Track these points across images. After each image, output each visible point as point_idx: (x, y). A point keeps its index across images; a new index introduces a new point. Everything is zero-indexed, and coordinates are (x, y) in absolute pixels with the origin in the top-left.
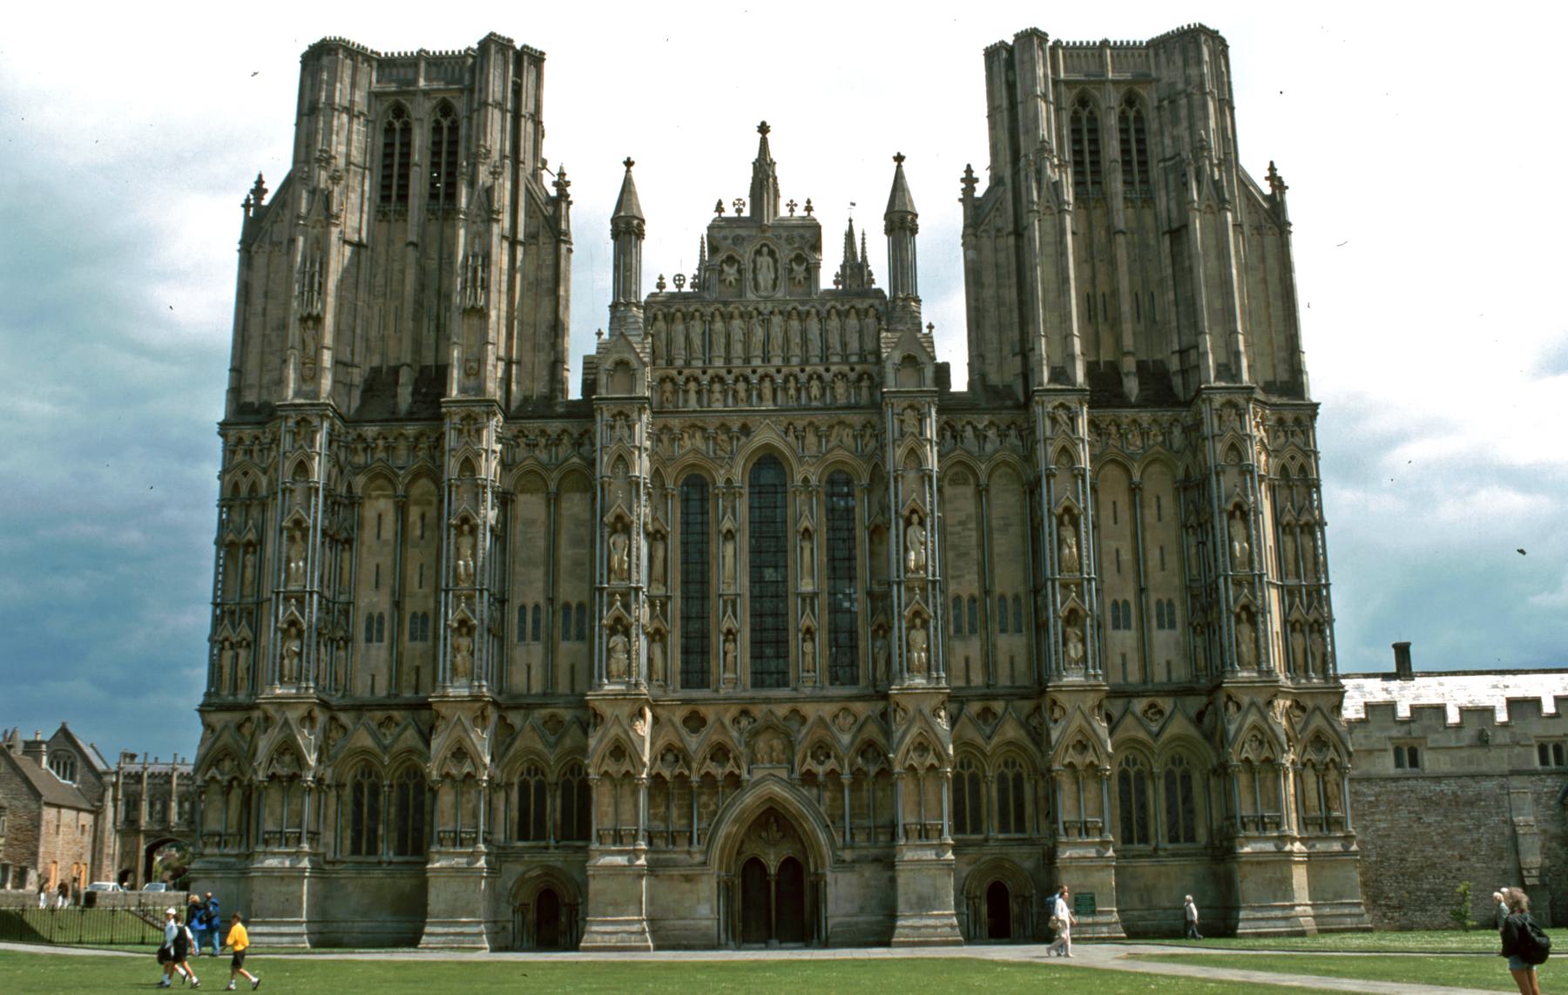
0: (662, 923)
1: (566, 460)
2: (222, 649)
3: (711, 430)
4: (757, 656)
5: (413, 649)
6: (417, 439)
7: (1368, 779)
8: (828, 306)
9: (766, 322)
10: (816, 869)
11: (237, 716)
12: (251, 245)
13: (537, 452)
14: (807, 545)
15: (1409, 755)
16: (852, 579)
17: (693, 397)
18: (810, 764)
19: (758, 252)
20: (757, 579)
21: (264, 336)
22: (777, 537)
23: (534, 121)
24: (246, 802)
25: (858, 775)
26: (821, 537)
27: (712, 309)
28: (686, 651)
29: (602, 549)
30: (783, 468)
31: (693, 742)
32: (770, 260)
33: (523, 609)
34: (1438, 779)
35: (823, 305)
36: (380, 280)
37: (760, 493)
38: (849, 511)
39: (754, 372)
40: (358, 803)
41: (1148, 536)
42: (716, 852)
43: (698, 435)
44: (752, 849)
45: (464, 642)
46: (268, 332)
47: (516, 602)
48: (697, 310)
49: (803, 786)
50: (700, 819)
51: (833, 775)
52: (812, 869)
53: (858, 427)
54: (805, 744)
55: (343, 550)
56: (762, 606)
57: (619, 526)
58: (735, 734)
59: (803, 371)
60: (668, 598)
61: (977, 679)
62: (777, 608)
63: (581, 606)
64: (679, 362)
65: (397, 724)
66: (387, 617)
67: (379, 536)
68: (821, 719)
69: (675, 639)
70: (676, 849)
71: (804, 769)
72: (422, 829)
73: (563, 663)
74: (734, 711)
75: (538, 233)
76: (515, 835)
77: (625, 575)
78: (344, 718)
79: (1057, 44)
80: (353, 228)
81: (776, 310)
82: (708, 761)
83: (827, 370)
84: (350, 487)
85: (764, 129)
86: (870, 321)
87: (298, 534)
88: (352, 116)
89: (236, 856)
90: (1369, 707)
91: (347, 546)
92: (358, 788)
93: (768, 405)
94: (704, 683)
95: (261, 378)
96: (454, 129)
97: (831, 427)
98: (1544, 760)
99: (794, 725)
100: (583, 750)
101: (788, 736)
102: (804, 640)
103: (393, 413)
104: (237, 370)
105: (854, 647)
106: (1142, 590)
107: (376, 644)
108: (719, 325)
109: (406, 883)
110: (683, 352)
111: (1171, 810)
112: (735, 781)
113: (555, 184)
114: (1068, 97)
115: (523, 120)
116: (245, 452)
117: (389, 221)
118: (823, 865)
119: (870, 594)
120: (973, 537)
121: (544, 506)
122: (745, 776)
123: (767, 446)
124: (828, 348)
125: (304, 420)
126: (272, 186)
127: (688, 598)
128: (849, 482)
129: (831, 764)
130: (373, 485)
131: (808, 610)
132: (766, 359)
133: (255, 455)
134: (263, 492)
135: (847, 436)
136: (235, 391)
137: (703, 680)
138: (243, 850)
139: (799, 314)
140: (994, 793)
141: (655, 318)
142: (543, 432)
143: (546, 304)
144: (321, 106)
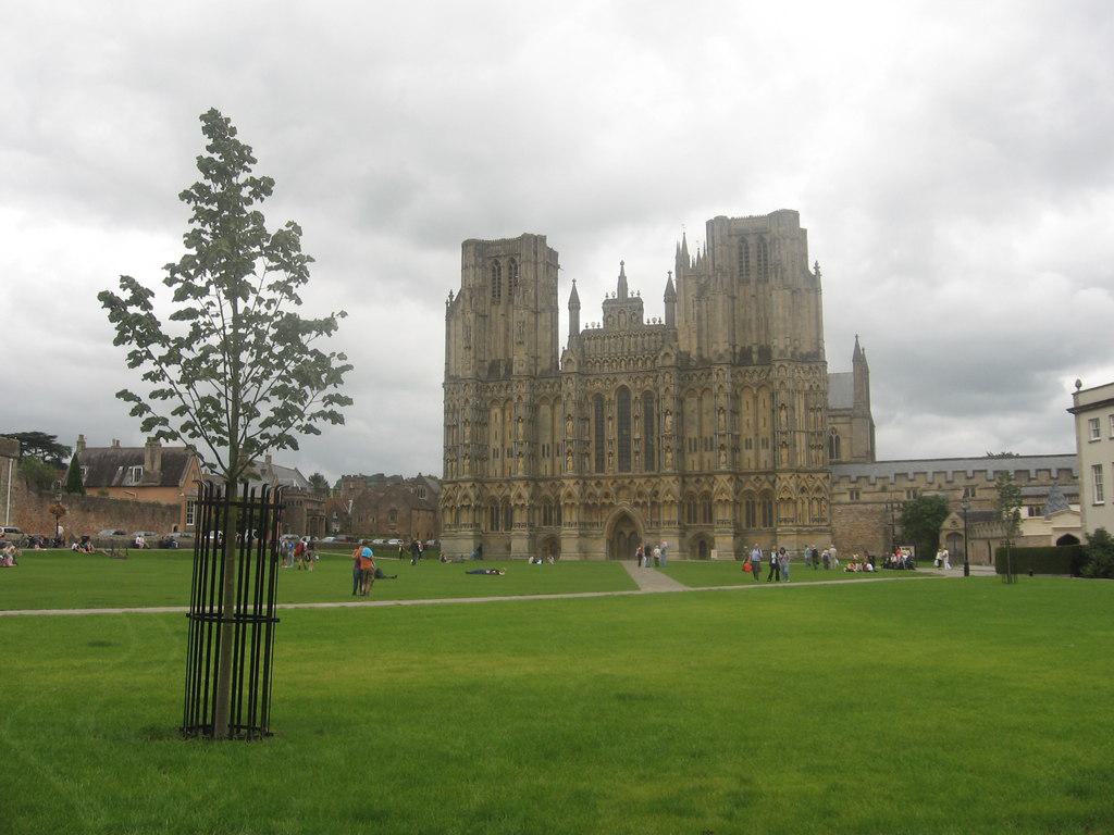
5: (509, 461)
7: (839, 504)
15: (855, 493)
17: (598, 368)
18: (638, 499)
19: (620, 313)
24: (457, 514)
25: (653, 503)
31: (599, 492)
33: (544, 446)
34: (865, 503)
40: (492, 513)
41: (760, 415)
45: (521, 460)
61: (697, 468)
69: (593, 455)
73: (557, 463)
79: (733, 218)
85: (622, 263)
86: (660, 337)
90: (842, 477)
92: (492, 508)
93: (623, 369)
94: (603, 471)
96: (516, 268)
98: (909, 497)
101: (629, 489)
106: (757, 435)
111: (764, 516)
114: (735, 240)
120: (696, 417)
126: (455, 294)
134: (457, 407)
135: (650, 381)
140: (702, 509)
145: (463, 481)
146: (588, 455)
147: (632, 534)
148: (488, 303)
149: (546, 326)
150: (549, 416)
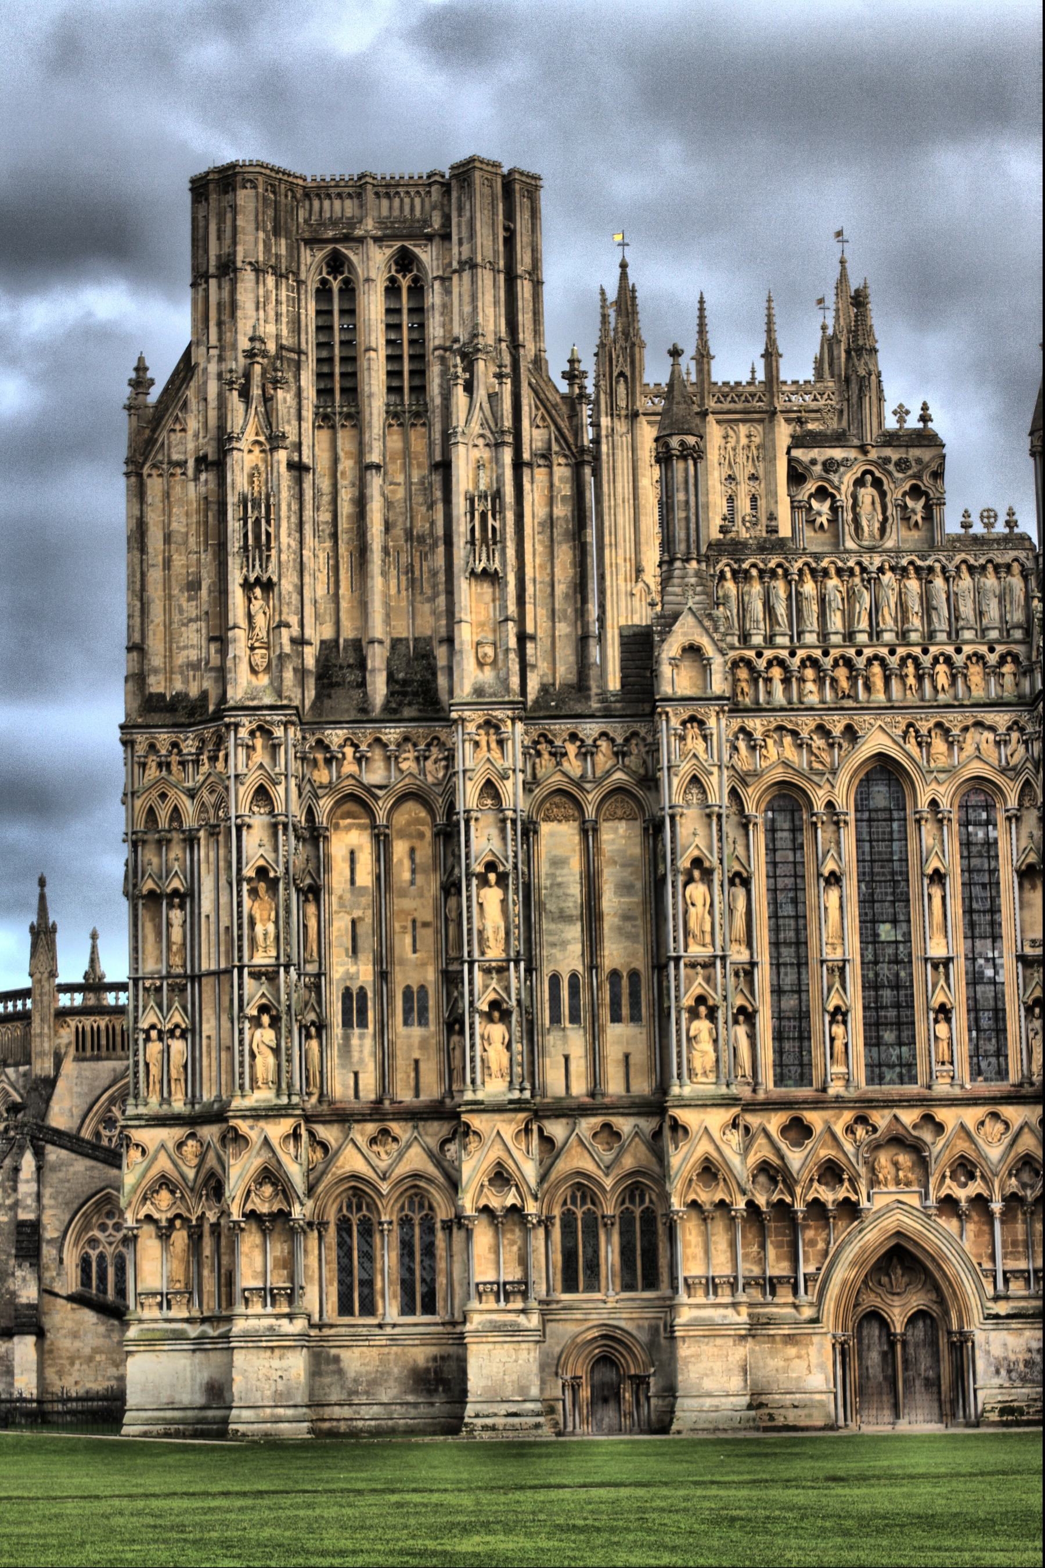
0: (764, 1399)
1: (608, 773)
2: (148, 1039)
3: (804, 734)
4: (872, 1041)
6: (398, 745)
8: (958, 558)
9: (872, 581)
10: (961, 1327)
11: (178, 1133)
12: (144, 464)
13: (566, 765)
14: (936, 892)
16: (996, 938)
17: (778, 688)
18: (951, 1188)
19: (859, 482)
20: (869, 938)
21: (169, 597)
22: (895, 882)
23: (532, 281)
25: (1012, 1200)
26: (955, 883)
27: (799, 564)
28: (779, 1036)
29: (675, 905)
30: (900, 785)
31: (795, 1158)
32: (875, 493)
33: (555, 980)
35: (950, 559)
36: (325, 516)
37: (870, 820)
38: (991, 845)
39: (859, 653)
40: (344, 1247)
42: (830, 1305)
43: (788, 740)
44: (871, 1300)
45: (497, 1031)
46: (175, 592)
47: (547, 971)
48: (779, 565)
49: (939, 1216)
50: (806, 1260)
51: (980, 1202)
52: (955, 1327)
53: (1002, 730)
54: (945, 1159)
55: (306, 900)
56: (877, 975)
57: (696, 874)
58: (849, 1148)
59: (925, 651)
60: (753, 964)
62: (897, 975)
63: (634, 975)
64: (757, 640)
65: (395, 1140)
66: (370, 995)
67: (353, 881)
68: (962, 1126)
69: (765, 1022)
70: (777, 1300)
71: (943, 1193)
72: (433, 1280)
74: (848, 1116)
75: (550, 448)
76: (559, 1285)
77: (708, 939)
78: (324, 1132)
80: (293, 444)
81: (887, 567)
82: (816, 1184)
83: (959, 651)
84: (310, 813)
86: (1016, 582)
87: (262, 886)
88: (279, 276)
89: (188, 1320)
91: (310, 896)
92: (344, 1226)
93: (880, 697)
94: (804, 1079)
95: (169, 655)
96: (417, 290)
97: (966, 729)
99: (927, 1136)
100: (662, 1175)
101: (917, 1149)
102: (936, 1021)
103: (364, 710)
104: (137, 648)
105: (1000, 1031)
107: (357, 1031)
108: (809, 587)
109: (420, 1355)
110: (762, 625)
112: (850, 1209)
113: (565, 375)
115: (519, 281)
116: (160, 765)
117: (333, 427)
118: (969, 1323)
119: (1021, 958)
121: (577, 839)
122: (864, 1204)
123: (882, 758)
124: (957, 619)
125: (260, 728)
126: (161, 374)
127: (778, 966)
128: (989, 807)
129: (975, 1188)
130: (339, 812)
131: (942, 982)
132: (875, 633)
133: (174, 768)
136: (137, 679)
137: (802, 1075)
138: (196, 1313)
139: (918, 570)
141: (722, 576)
142: (573, 737)
143: (564, 554)
144: (239, 264)
145: (257, 1115)
146: (747, 1015)
147: (912, 1320)
148: (308, 414)
149: (550, 521)
150: (575, 865)
